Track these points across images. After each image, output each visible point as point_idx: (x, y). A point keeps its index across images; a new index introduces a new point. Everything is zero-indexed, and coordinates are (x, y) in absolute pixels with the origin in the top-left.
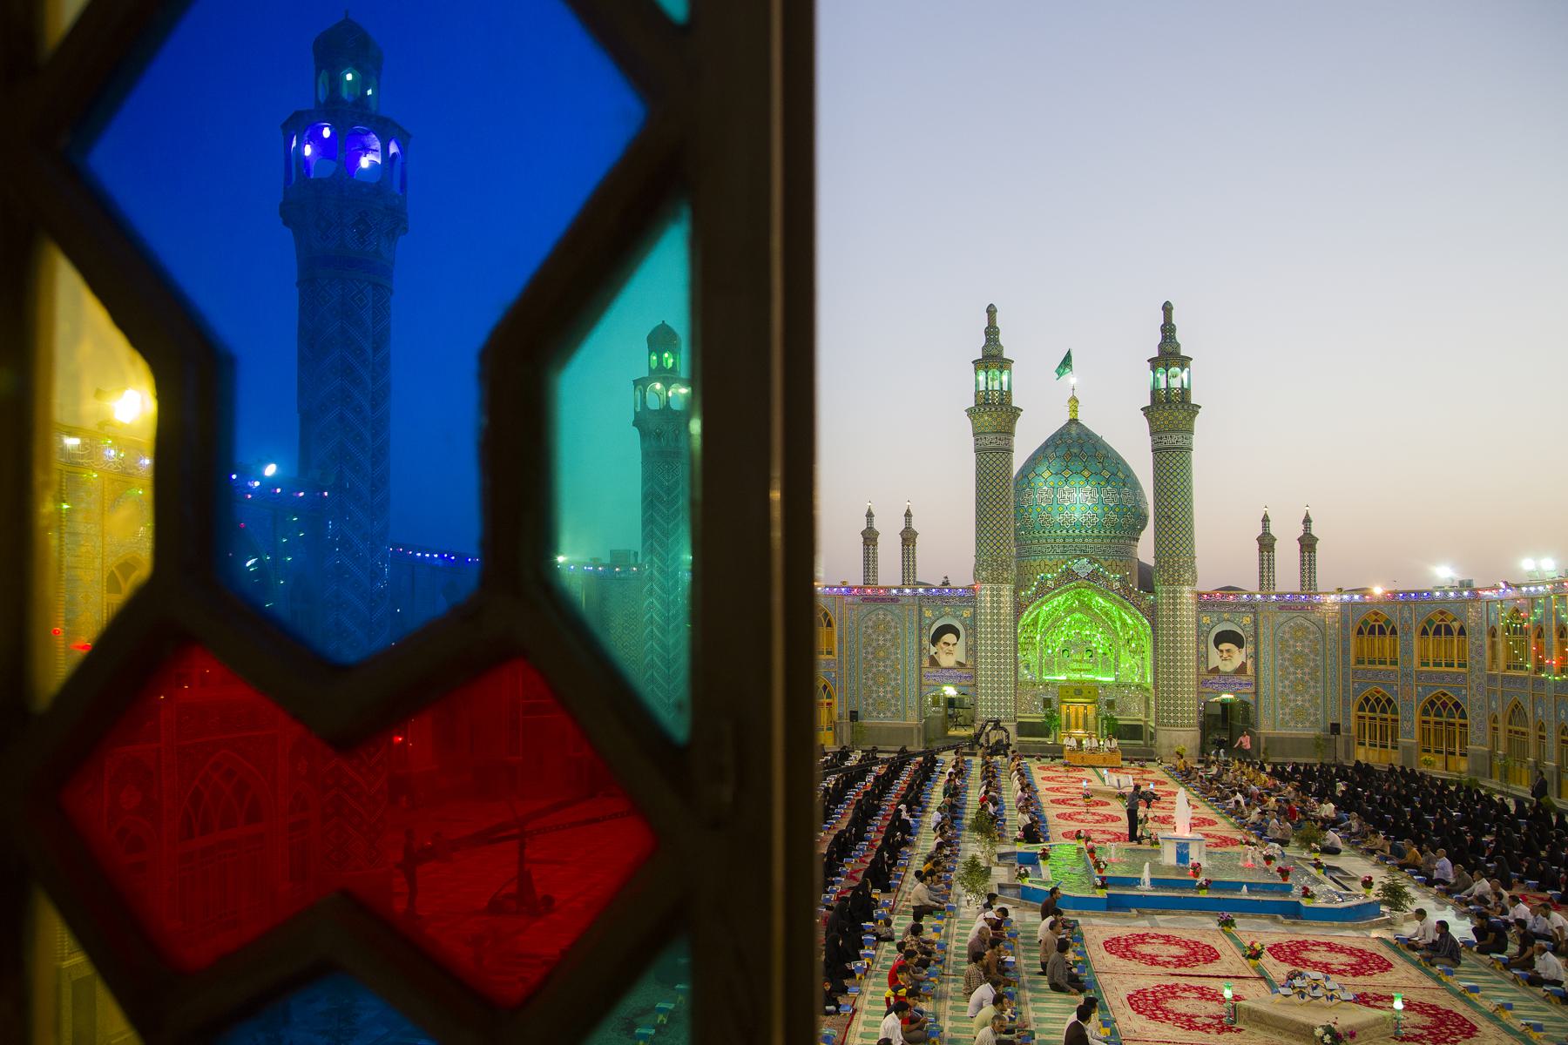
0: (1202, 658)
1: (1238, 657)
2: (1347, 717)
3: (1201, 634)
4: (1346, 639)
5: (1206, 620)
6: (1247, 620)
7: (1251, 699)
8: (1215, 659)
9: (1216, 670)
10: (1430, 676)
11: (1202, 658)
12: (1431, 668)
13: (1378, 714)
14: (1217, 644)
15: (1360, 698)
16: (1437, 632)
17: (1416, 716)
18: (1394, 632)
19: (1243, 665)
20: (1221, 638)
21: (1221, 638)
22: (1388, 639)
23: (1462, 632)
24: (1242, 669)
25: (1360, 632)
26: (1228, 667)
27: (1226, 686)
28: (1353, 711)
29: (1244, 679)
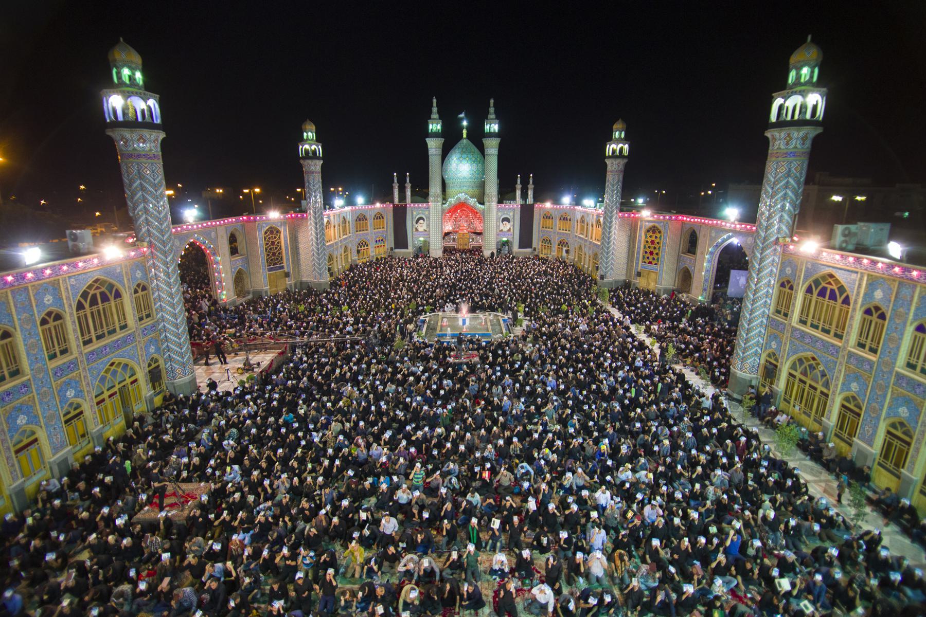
0: (498, 226)
1: (508, 226)
3: (498, 219)
6: (512, 214)
8: (502, 227)
10: (560, 234)
11: (498, 226)
17: (556, 246)
20: (504, 220)
21: (504, 220)
24: (509, 230)
26: (505, 229)
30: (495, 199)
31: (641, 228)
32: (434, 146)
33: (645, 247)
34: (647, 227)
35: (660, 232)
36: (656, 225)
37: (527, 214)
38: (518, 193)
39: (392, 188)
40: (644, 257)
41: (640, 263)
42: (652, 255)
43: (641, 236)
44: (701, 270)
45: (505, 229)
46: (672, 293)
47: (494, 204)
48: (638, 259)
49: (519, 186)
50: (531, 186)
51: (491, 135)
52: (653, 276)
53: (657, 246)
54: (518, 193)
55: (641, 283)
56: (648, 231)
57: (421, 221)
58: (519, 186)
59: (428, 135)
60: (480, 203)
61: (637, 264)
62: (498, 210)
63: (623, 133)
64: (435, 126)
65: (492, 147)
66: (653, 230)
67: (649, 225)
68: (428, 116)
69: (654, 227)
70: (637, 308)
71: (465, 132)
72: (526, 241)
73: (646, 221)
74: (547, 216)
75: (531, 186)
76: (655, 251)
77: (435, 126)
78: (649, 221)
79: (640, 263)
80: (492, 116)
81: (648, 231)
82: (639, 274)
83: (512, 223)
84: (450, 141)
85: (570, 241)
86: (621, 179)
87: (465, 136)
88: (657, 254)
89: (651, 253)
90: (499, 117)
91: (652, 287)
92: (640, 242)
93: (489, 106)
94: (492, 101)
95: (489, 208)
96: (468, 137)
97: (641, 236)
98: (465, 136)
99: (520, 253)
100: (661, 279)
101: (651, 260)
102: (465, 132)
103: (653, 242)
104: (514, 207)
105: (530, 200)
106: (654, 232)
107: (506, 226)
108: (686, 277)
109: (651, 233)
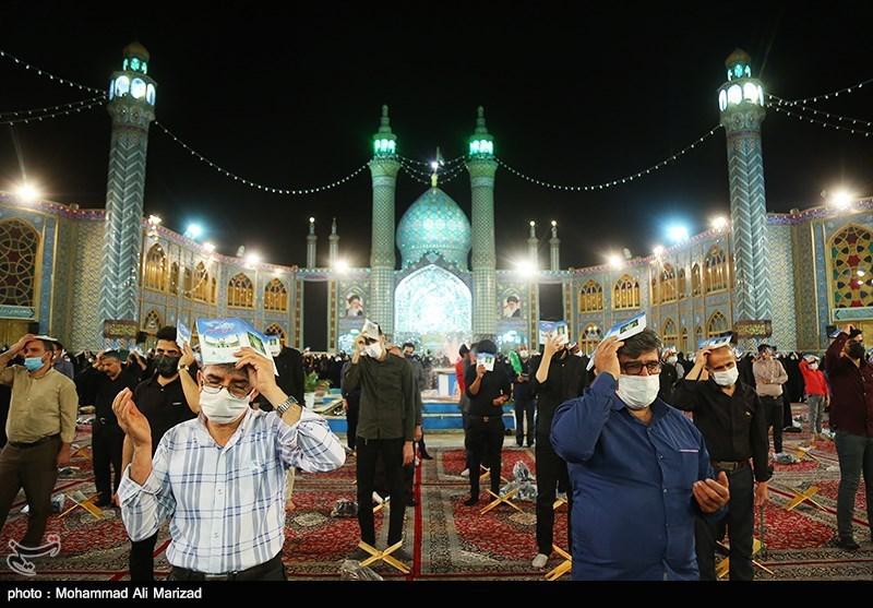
12: (621, 308)
16: (624, 287)
18: (600, 290)
22: (597, 294)
23: (637, 285)
25: (583, 292)
30: (492, 262)
32: (381, 178)
39: (305, 243)
51: (476, 158)
57: (356, 300)
62: (499, 279)
63: (748, 70)
64: (384, 145)
65: (483, 182)
68: (374, 129)
71: (434, 178)
77: (384, 145)
80: (481, 130)
84: (408, 192)
86: (760, 147)
87: (434, 183)
90: (494, 132)
96: (439, 186)
98: (434, 183)
102: (434, 178)
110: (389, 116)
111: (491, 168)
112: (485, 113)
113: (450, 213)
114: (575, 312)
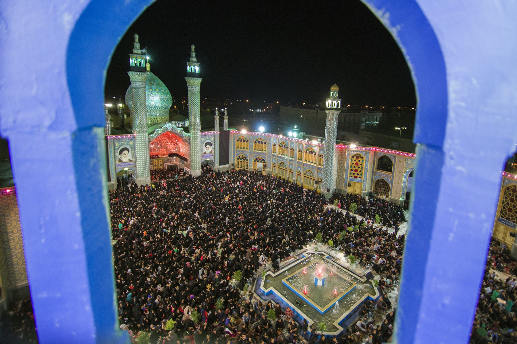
0: (202, 150)
1: (211, 148)
2: (234, 161)
3: (202, 143)
4: (234, 142)
5: (203, 139)
6: (213, 139)
7: (213, 159)
8: (205, 150)
9: (205, 153)
11: (202, 150)
13: (242, 161)
14: (206, 145)
15: (238, 157)
19: (212, 151)
24: (211, 152)
26: (208, 152)
27: (208, 157)
28: (236, 160)
29: (212, 154)
30: (199, 128)
31: (348, 155)
33: (351, 167)
34: (353, 155)
35: (362, 158)
36: (360, 153)
37: (225, 138)
38: (217, 122)
40: (351, 173)
41: (349, 177)
42: (357, 172)
43: (349, 161)
44: (399, 183)
45: (208, 152)
46: (370, 195)
47: (199, 132)
48: (347, 175)
49: (217, 118)
50: (226, 117)
51: (193, 75)
52: (358, 185)
53: (360, 166)
54: (217, 122)
55: (350, 190)
56: (353, 157)
58: (217, 118)
59: (129, 68)
60: (186, 132)
61: (347, 178)
62: (202, 136)
66: (357, 156)
67: (354, 153)
69: (358, 154)
70: (239, 176)
72: (224, 159)
73: (352, 151)
74: (242, 140)
75: (226, 117)
76: (359, 170)
78: (354, 151)
79: (349, 177)
80: (195, 60)
81: (353, 157)
82: (349, 185)
83: (213, 146)
85: (267, 159)
88: (360, 171)
89: (356, 171)
91: (357, 191)
92: (348, 164)
93: (190, 50)
94: (193, 47)
95: (195, 136)
97: (349, 161)
99: (220, 168)
100: (363, 187)
101: (356, 175)
103: (357, 164)
104: (216, 132)
105: (226, 128)
106: (357, 157)
107: (209, 149)
108: (382, 186)
109: (355, 158)
110: (139, 42)
111: (198, 81)
112: (195, 49)
113: (163, 91)
114: (234, 148)
